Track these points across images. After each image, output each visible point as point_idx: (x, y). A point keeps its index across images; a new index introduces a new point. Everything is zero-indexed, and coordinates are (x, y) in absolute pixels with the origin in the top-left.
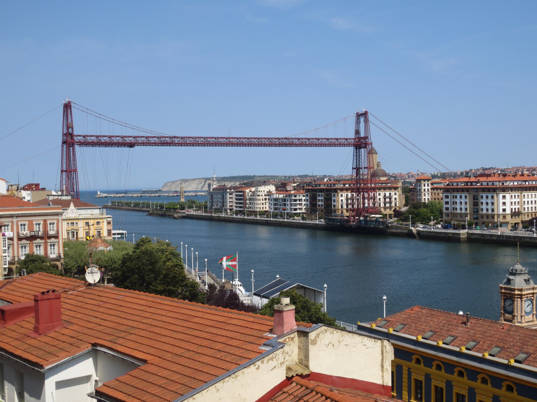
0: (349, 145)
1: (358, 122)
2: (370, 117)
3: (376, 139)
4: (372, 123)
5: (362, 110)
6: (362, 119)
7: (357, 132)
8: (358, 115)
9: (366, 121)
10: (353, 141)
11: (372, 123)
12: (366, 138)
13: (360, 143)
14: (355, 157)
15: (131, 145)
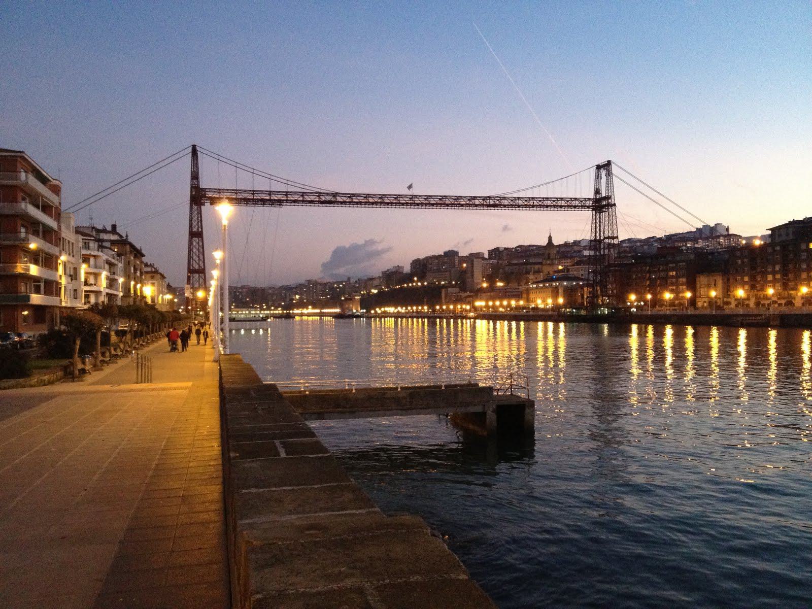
0: (583, 207)
1: (598, 177)
2: (614, 169)
3: (622, 197)
4: (616, 176)
5: (602, 161)
6: (603, 173)
7: (597, 192)
8: (599, 167)
9: (609, 174)
10: (591, 202)
11: (616, 176)
12: (608, 198)
13: (601, 204)
14: (594, 225)
15: (280, 202)
